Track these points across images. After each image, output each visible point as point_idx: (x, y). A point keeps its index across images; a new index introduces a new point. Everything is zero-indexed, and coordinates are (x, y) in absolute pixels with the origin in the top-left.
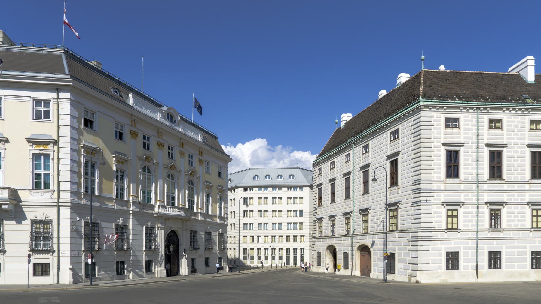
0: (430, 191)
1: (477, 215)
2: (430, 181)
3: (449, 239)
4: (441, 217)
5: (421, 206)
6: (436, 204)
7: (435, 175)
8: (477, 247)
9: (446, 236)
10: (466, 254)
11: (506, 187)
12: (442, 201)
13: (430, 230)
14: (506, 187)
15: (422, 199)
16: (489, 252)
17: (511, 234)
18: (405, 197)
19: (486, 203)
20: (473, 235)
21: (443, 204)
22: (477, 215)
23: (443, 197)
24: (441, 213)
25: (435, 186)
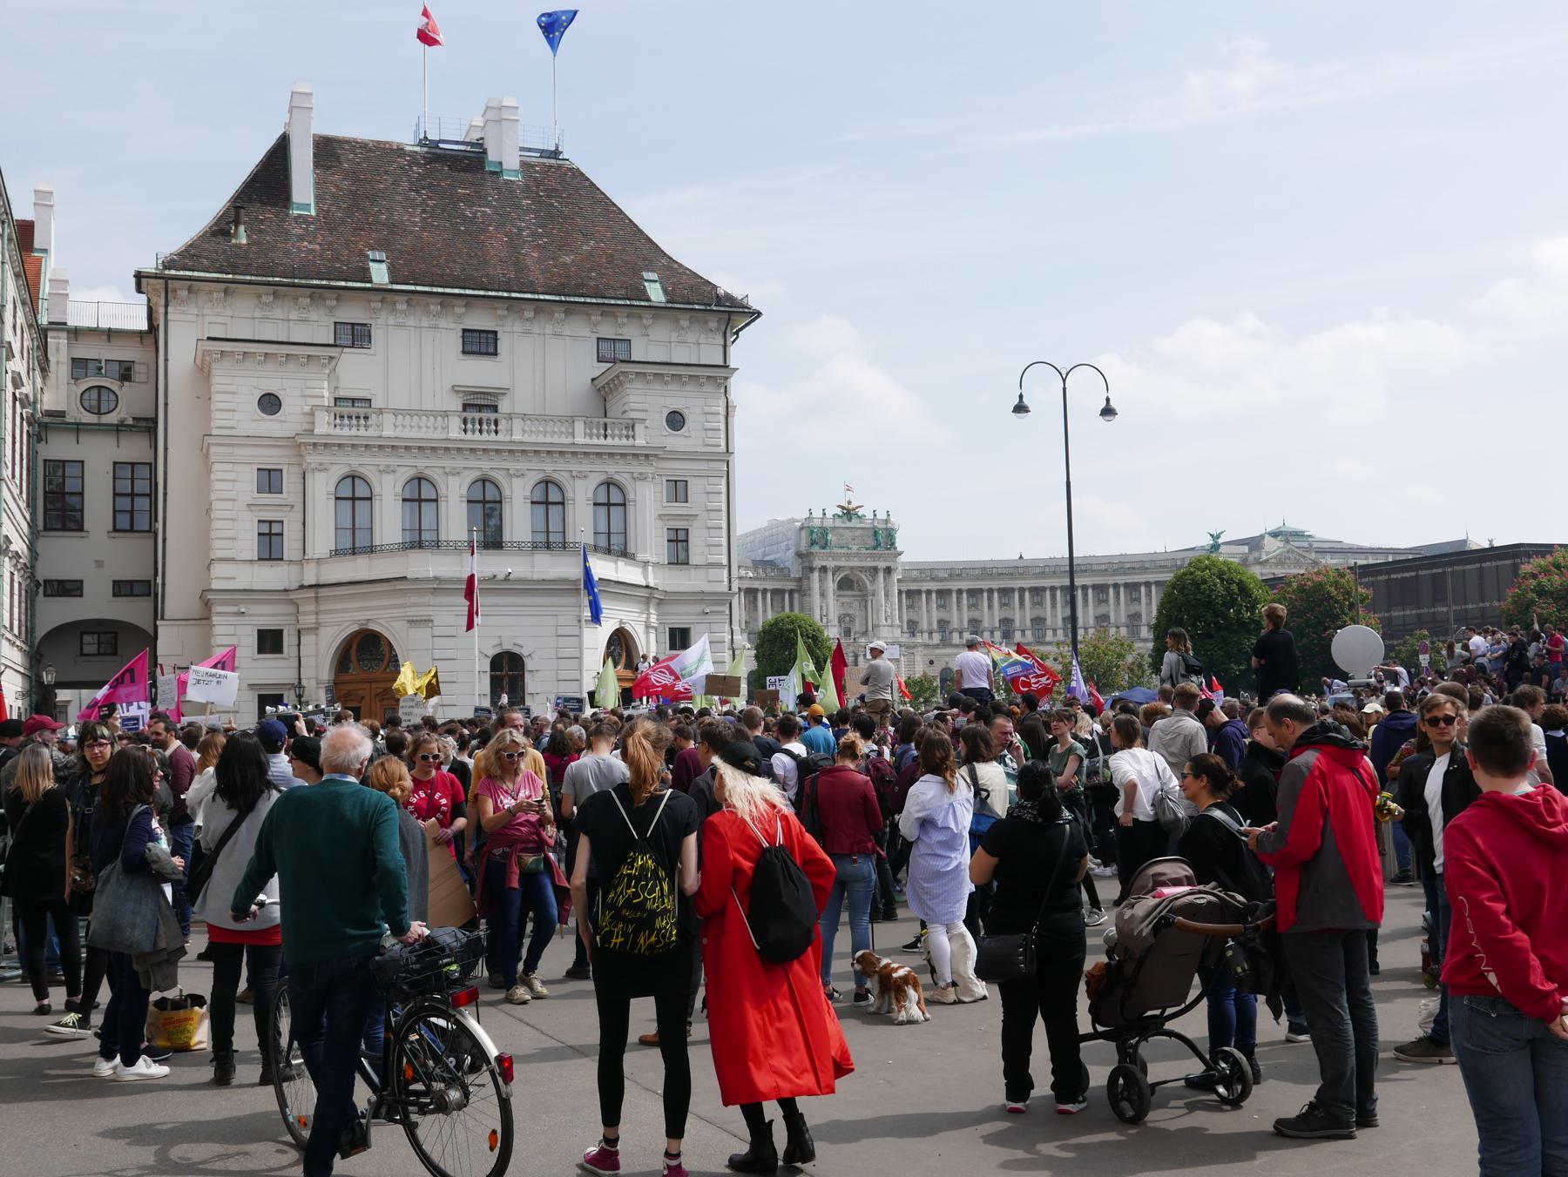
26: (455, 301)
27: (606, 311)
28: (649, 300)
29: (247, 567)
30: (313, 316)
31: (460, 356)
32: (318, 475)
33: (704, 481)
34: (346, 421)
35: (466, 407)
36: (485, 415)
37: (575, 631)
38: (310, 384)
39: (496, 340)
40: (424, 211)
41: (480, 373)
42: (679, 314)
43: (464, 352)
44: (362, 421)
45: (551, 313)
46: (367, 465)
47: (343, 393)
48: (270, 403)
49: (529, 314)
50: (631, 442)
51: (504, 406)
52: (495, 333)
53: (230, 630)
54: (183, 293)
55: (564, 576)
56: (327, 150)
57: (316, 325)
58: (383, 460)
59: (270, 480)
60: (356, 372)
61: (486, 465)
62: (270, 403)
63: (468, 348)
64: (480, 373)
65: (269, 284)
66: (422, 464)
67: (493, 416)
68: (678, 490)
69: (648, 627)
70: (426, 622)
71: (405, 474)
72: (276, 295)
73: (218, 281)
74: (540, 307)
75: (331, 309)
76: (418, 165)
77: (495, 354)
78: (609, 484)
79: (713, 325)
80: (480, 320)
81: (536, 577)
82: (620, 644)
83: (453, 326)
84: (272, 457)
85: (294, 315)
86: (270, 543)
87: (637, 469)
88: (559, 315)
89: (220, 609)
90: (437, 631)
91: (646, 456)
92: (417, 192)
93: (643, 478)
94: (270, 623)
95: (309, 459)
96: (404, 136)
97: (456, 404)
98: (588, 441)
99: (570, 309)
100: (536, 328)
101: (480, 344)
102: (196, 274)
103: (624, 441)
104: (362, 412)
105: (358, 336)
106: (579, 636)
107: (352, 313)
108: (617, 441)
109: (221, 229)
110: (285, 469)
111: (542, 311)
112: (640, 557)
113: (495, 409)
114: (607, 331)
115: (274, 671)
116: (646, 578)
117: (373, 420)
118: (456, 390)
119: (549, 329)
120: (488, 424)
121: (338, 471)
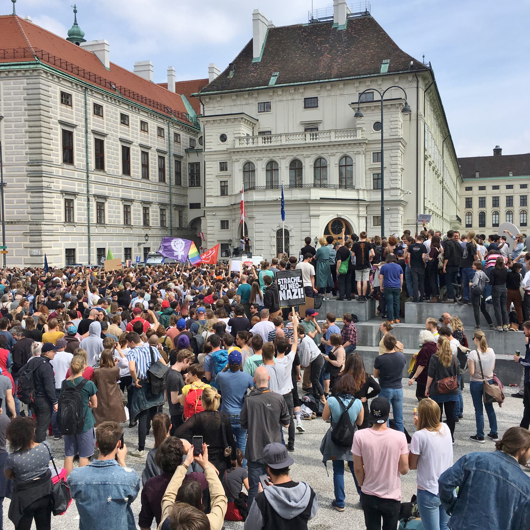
0: (50, 175)
1: (88, 209)
2: (50, 164)
3: (67, 234)
4: (59, 208)
5: (44, 194)
6: (56, 192)
7: (54, 157)
8: (89, 243)
9: (65, 230)
10: (81, 250)
11: (107, 180)
12: (61, 189)
13: (51, 222)
14: (107, 180)
15: (45, 184)
16: (66, 249)
17: (111, 230)
18: (15, 178)
19: (95, 196)
20: (84, 230)
21: (62, 192)
22: (88, 209)
23: (61, 185)
24: (60, 202)
25: (54, 169)
26: (300, 87)
27: (361, 80)
28: (379, 73)
29: (216, 198)
30: (250, 102)
31: (304, 109)
32: (236, 163)
33: (390, 151)
34: (266, 140)
35: (306, 130)
36: (314, 132)
37: (308, 220)
38: (236, 129)
39: (317, 100)
40: (302, 51)
41: (311, 115)
42: (407, 75)
43: (305, 108)
44: (269, 140)
45: (299, 89)
46: (252, 157)
47: (261, 130)
48: (223, 138)
49: (329, 88)
50: (355, 138)
51: (320, 128)
52: (317, 98)
53: (212, 221)
54: (207, 100)
55: (304, 198)
56: (274, 34)
57: (249, 106)
58: (258, 156)
59: (223, 167)
60: (266, 122)
61: (319, 152)
62: (223, 138)
63: (307, 106)
64: (311, 115)
65: (232, 92)
66: (271, 156)
67: (317, 132)
68: (379, 156)
69: (359, 216)
70: (251, 218)
71: (266, 160)
72: (237, 96)
73: (216, 94)
74: (333, 84)
75: (256, 98)
76: (305, 32)
77: (317, 107)
78: (346, 157)
79: (410, 79)
80: (310, 93)
81: (293, 199)
82: (338, 225)
83: (300, 97)
84: (223, 158)
85: (244, 102)
86: (224, 191)
87: (356, 149)
88: (341, 86)
89: (208, 213)
90: (257, 221)
91: (360, 143)
92: (302, 43)
93: (359, 153)
94: (224, 218)
95: (233, 157)
96: (305, 21)
97: (302, 129)
98: (312, 141)
99: (346, 83)
100: (333, 93)
101: (311, 103)
102: (210, 93)
103: (352, 138)
104: (269, 136)
105: (265, 107)
106: (310, 222)
107: (264, 99)
108: (320, 140)
109: (226, 73)
110: (228, 161)
111: (348, 84)
112: (356, 188)
113: (317, 129)
114: (362, 89)
115: (225, 235)
116: (359, 196)
117: (273, 139)
118: (302, 123)
119: (338, 92)
120: (268, 139)
121: (242, 161)
